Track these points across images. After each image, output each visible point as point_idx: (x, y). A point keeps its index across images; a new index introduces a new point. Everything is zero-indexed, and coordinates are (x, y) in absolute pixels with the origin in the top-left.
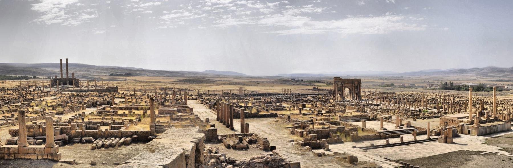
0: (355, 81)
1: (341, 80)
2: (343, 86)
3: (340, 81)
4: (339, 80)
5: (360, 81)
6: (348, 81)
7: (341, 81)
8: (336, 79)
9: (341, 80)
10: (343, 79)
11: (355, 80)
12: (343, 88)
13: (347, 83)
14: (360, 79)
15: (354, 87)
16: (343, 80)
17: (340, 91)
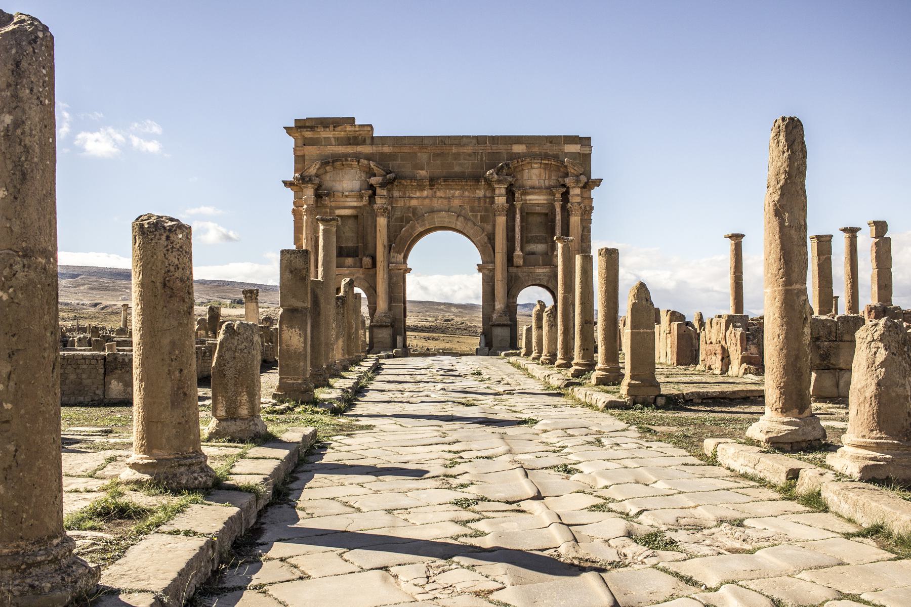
0: (517, 156)
1: (367, 149)
2: (379, 201)
3: (357, 157)
4: (349, 149)
5: (585, 159)
6: (441, 155)
7: (369, 157)
8: (308, 134)
9: (367, 149)
10: (384, 140)
11: (519, 148)
12: (382, 221)
13: (433, 181)
14: (585, 141)
15: (501, 220)
16: (386, 150)
17: (349, 261)
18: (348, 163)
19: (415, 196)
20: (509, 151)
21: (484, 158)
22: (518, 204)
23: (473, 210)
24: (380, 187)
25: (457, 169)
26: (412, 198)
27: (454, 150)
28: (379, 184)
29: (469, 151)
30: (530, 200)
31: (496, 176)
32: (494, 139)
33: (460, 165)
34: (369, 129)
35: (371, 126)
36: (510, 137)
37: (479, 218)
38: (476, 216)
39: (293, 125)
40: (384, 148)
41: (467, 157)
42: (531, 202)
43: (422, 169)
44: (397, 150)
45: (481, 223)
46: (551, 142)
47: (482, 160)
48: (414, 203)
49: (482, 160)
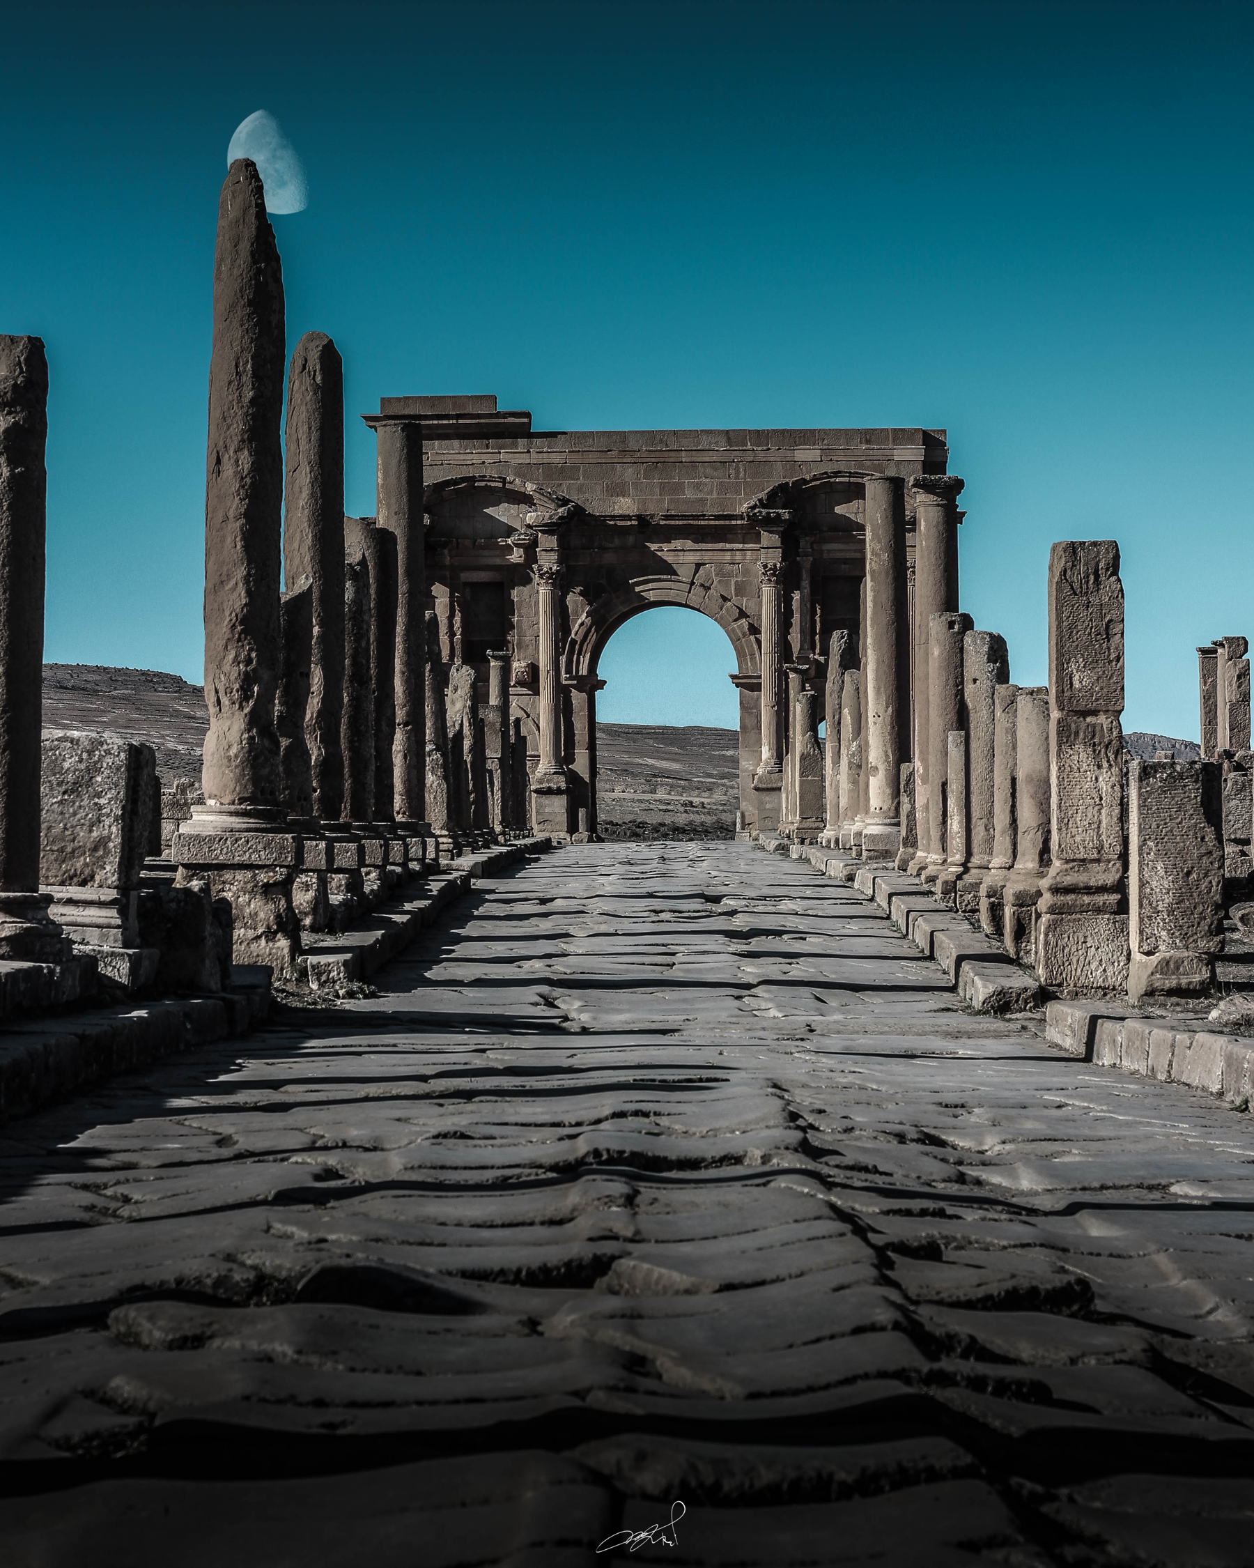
7: (524, 471)
18: (483, 484)
19: (612, 546)
20: (788, 459)
21: (742, 475)
22: (807, 562)
23: (720, 573)
24: (543, 532)
25: (689, 494)
26: (604, 549)
27: (684, 457)
28: (544, 525)
29: (714, 459)
30: (829, 551)
31: (764, 511)
32: (761, 436)
33: (697, 487)
34: (525, 420)
35: (528, 415)
36: (790, 432)
37: (733, 588)
38: (727, 583)
39: (377, 412)
40: (553, 455)
41: (709, 471)
42: (832, 556)
43: (623, 493)
44: (576, 459)
45: (736, 596)
46: (868, 442)
47: (737, 477)
48: (609, 558)
49: (737, 477)
